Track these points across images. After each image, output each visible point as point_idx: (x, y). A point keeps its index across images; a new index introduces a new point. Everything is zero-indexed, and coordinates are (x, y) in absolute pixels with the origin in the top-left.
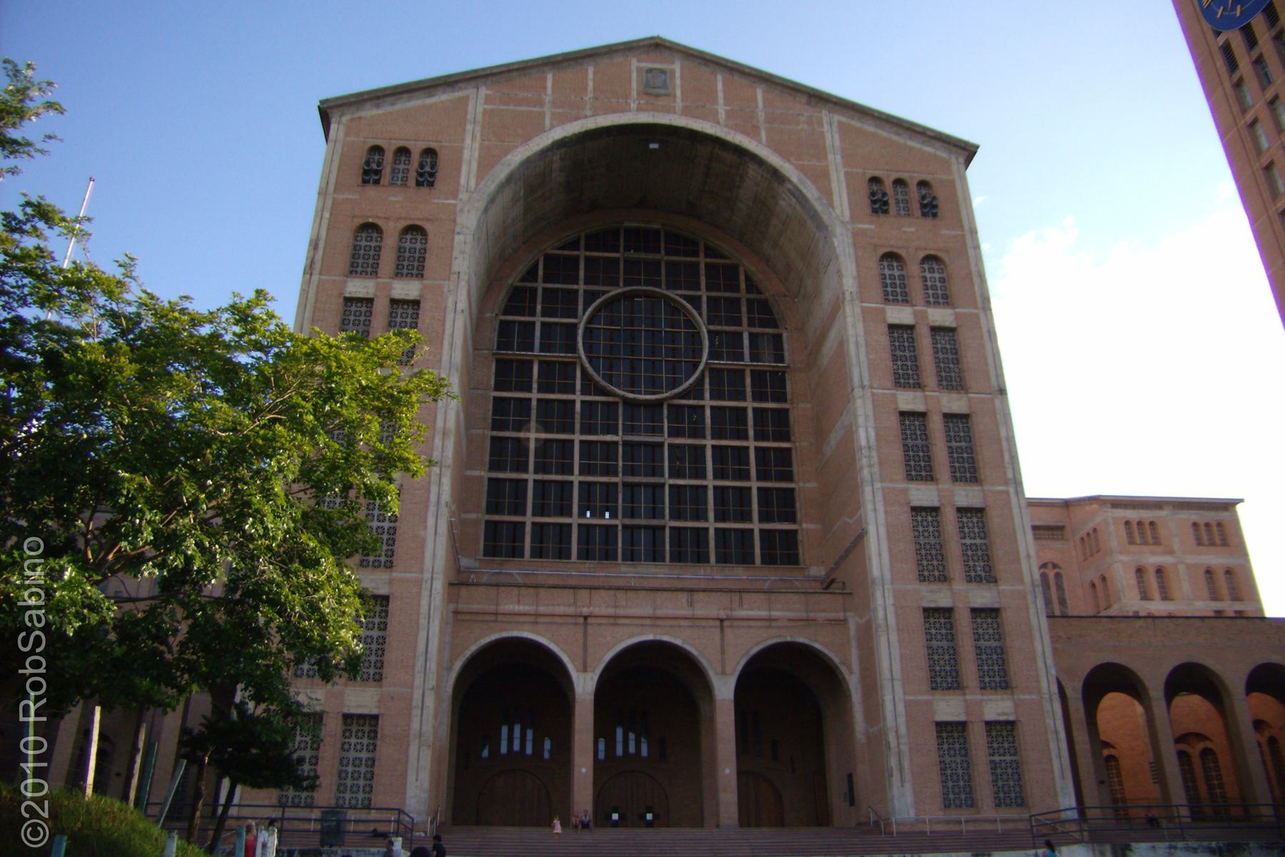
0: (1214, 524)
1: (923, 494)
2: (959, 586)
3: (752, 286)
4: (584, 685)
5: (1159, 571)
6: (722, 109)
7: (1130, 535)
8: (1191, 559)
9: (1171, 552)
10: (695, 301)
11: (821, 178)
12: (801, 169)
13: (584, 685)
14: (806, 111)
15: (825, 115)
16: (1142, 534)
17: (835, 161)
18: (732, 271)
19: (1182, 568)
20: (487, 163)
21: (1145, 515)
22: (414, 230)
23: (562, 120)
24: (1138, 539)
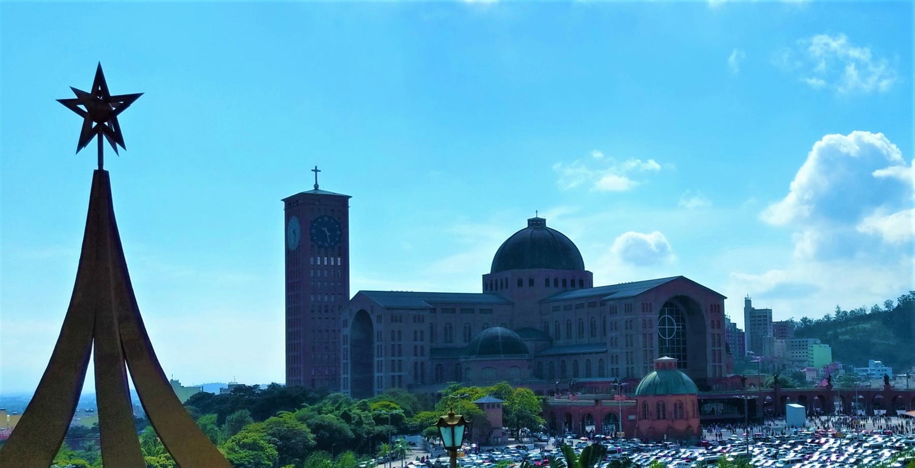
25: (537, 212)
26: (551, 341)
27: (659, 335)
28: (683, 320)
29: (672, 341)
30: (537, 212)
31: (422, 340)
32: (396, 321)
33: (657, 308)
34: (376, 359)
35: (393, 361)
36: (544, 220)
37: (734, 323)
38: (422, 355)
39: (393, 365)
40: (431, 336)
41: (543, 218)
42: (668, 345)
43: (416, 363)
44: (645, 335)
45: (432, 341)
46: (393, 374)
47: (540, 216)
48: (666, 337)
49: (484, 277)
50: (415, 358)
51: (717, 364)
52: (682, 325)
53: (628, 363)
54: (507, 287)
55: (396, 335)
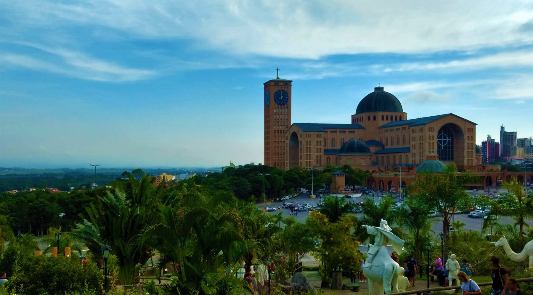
26: (383, 146)
27: (438, 144)
28: (452, 136)
29: (445, 147)
30: (379, 84)
31: (320, 145)
32: (308, 137)
33: (437, 129)
34: (299, 154)
35: (307, 155)
36: (383, 88)
37: (493, 139)
38: (320, 152)
39: (307, 157)
40: (325, 144)
41: (382, 87)
42: (443, 148)
43: (317, 156)
44: (429, 143)
45: (325, 146)
47: (381, 86)
48: (442, 144)
49: (352, 116)
51: (470, 158)
52: (451, 139)
53: (420, 157)
54: (363, 120)
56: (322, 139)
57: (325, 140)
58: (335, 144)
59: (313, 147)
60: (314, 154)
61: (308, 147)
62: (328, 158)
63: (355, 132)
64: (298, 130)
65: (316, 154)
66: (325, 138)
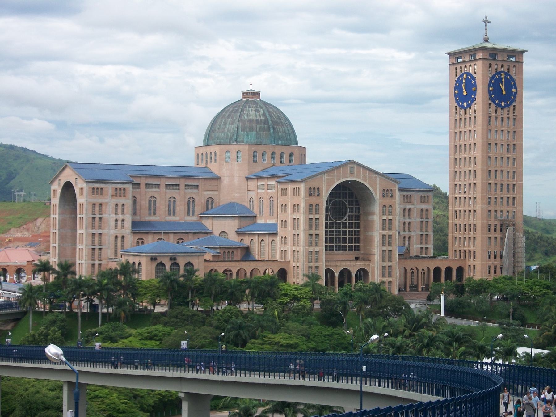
0: (426, 196)
1: (384, 248)
2: (387, 262)
3: (356, 197)
4: (337, 275)
5: (410, 210)
6: (362, 175)
7: (404, 199)
8: (418, 207)
9: (413, 205)
10: (346, 201)
11: (375, 190)
12: (372, 188)
13: (337, 275)
14: (375, 175)
15: (377, 176)
16: (407, 199)
17: (378, 186)
18: (352, 194)
19: (415, 209)
20: (327, 191)
21: (409, 193)
22: (317, 205)
23: (338, 180)
24: (406, 201)
25: (251, 84)
35: (94, 234)
36: (258, 94)
43: (116, 237)
45: (134, 213)
46: (93, 247)
47: (255, 88)
50: (116, 232)
55: (97, 208)
56: (128, 202)
57: (135, 202)
58: (155, 210)
59: (109, 216)
60: (109, 232)
61: (98, 216)
62: (140, 241)
63: (200, 187)
64: (76, 179)
65: (113, 232)
66: (134, 197)
